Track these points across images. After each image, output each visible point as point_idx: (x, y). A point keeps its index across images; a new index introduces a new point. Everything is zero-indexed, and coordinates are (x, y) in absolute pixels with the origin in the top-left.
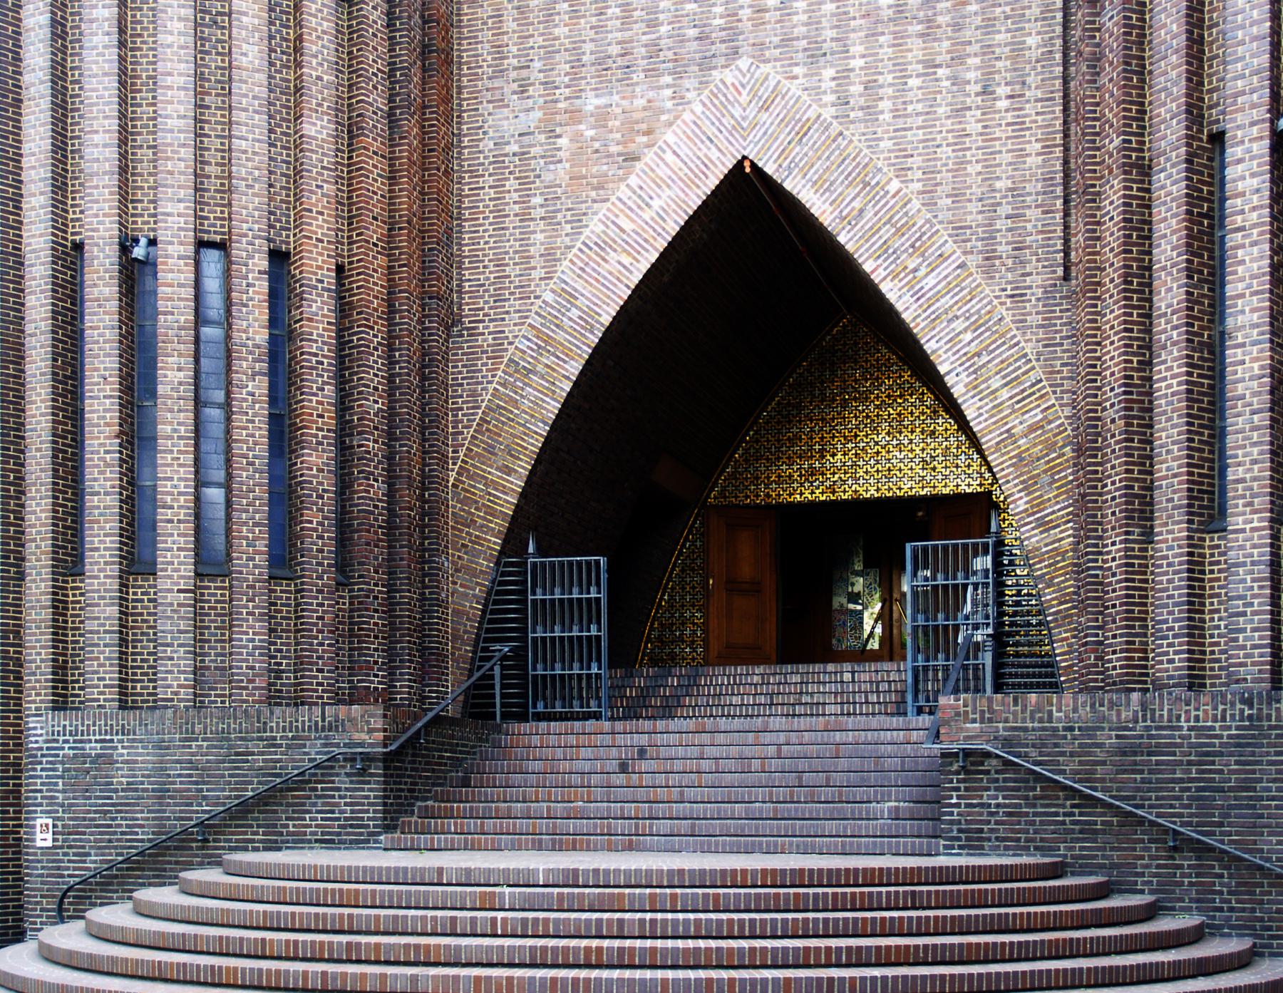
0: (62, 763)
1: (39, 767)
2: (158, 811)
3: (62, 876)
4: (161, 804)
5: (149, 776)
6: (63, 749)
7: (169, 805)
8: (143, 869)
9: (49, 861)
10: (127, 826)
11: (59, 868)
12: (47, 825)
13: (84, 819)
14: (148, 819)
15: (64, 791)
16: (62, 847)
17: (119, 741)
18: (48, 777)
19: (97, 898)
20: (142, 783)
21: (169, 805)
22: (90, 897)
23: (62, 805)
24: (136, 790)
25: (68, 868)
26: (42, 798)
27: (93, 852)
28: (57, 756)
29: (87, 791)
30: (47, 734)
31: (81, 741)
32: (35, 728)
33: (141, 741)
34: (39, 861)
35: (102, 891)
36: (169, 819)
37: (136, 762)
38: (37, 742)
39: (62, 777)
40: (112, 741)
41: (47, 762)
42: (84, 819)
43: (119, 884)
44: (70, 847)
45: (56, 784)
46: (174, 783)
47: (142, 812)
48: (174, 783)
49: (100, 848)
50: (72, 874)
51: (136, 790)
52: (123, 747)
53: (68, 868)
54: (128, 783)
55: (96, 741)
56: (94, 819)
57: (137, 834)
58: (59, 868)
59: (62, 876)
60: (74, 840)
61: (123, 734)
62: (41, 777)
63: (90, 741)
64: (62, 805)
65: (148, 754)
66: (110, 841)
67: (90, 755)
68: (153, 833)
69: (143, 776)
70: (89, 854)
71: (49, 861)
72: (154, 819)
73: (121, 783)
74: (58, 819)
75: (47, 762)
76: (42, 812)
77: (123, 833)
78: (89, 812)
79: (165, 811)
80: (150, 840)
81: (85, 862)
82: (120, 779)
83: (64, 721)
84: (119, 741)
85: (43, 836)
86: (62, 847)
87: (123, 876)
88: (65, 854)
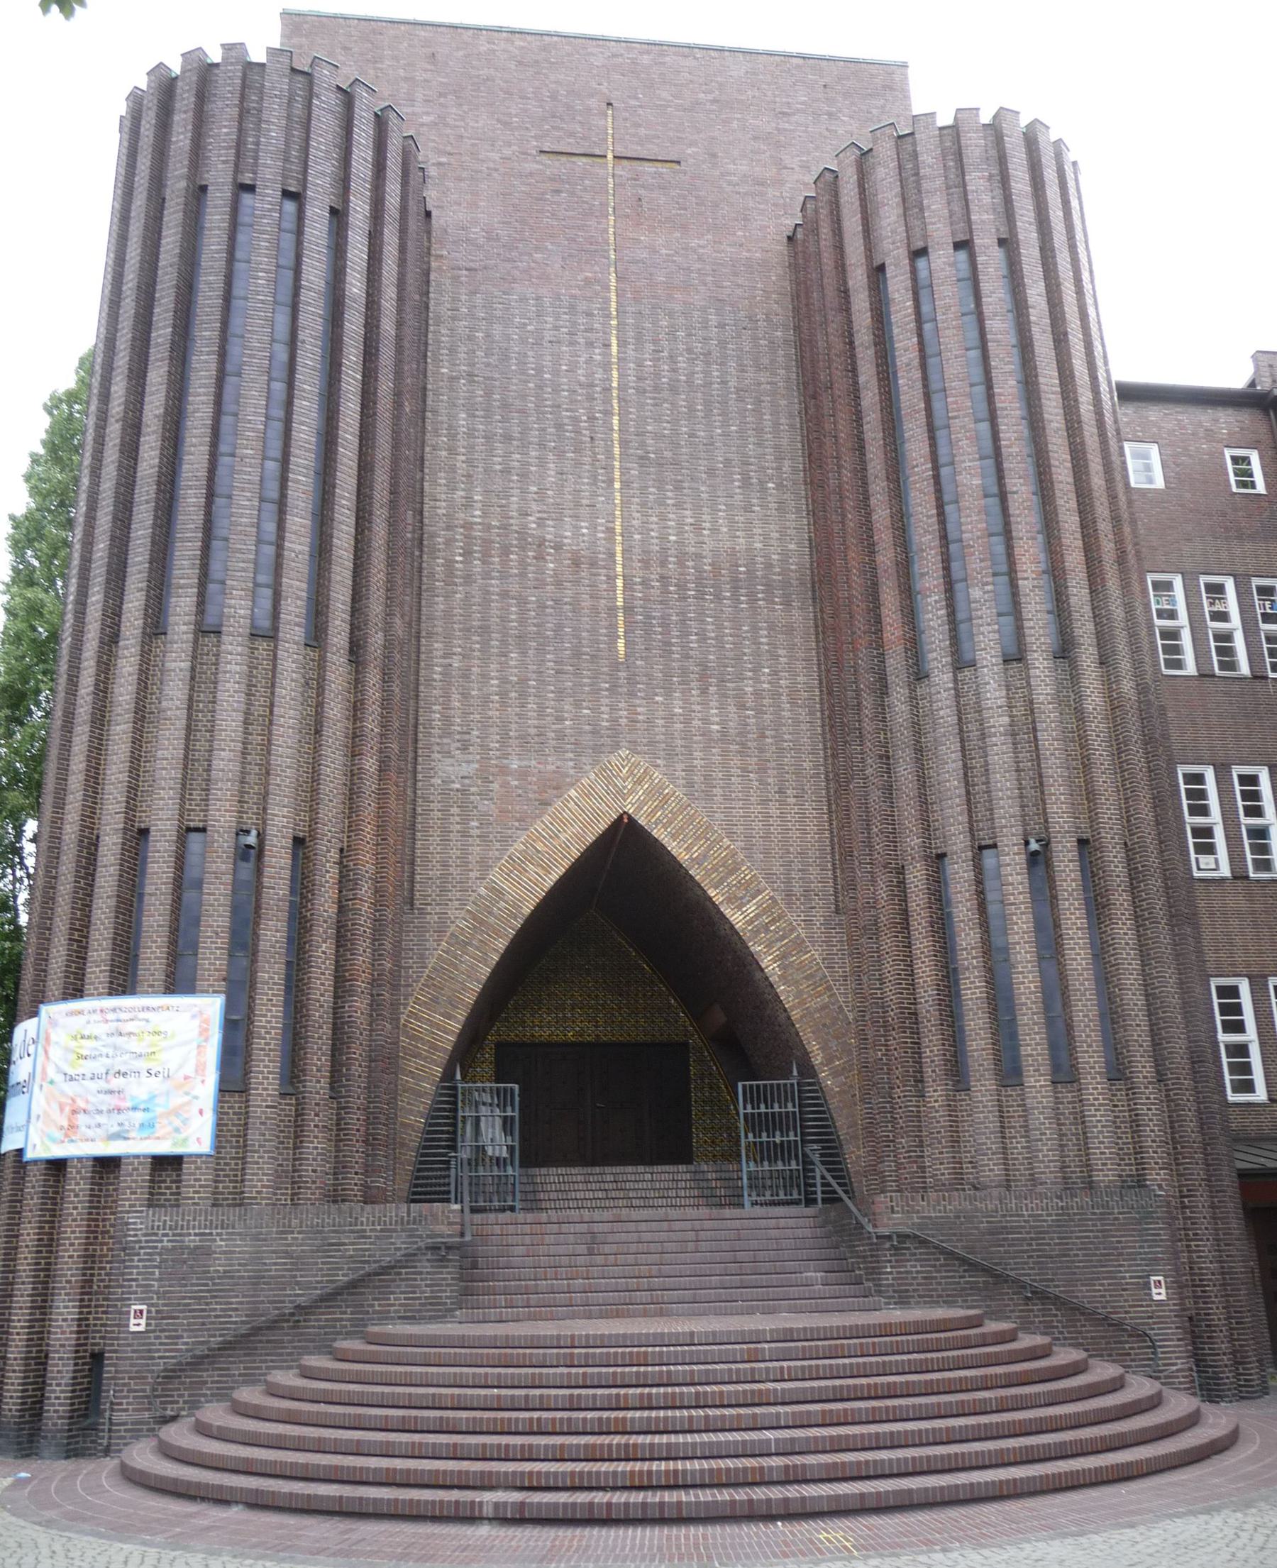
0: (160, 1254)
1: (136, 1258)
2: (253, 1296)
3: (153, 1358)
4: (255, 1290)
5: (246, 1265)
6: (162, 1241)
7: (263, 1290)
8: (234, 1349)
9: (140, 1345)
10: (222, 1310)
11: (149, 1351)
12: (141, 1312)
13: (179, 1305)
14: (241, 1303)
15: (160, 1280)
16: (154, 1331)
17: (218, 1234)
18: (145, 1267)
19: (186, 1377)
20: (239, 1271)
21: (263, 1290)
22: (180, 1377)
23: (157, 1293)
24: (232, 1277)
25: (159, 1351)
26: (137, 1286)
27: (185, 1334)
28: (156, 1247)
29: (184, 1279)
30: (147, 1228)
31: (180, 1235)
32: (135, 1223)
33: (240, 1234)
34: (129, 1345)
35: (192, 1370)
36: (263, 1302)
37: (234, 1252)
38: (136, 1235)
39: (158, 1267)
40: (211, 1234)
41: (145, 1254)
42: (179, 1305)
43: (210, 1363)
44: (161, 1331)
45: (153, 1273)
46: (270, 1270)
47: (237, 1296)
48: (270, 1270)
49: (192, 1331)
50: (165, 1355)
51: (232, 1277)
52: (222, 1240)
53: (159, 1351)
54: (225, 1272)
55: (196, 1235)
56: (189, 1304)
57: (230, 1316)
58: (149, 1351)
59: (153, 1358)
60: (167, 1324)
61: (222, 1228)
62: (137, 1267)
63: (190, 1235)
64: (157, 1293)
65: (246, 1246)
66: (203, 1324)
67: (188, 1247)
68: (247, 1316)
69: (240, 1265)
70: (182, 1337)
71: (140, 1345)
72: (248, 1303)
73: (218, 1271)
74: (153, 1305)
75: (145, 1254)
76: (136, 1299)
77: (216, 1317)
78: (184, 1298)
79: (259, 1296)
80: (242, 1322)
81: (176, 1344)
82: (218, 1266)
83: (164, 1217)
84: (218, 1234)
85: (137, 1321)
86: (154, 1331)
87: (214, 1356)
88: (157, 1338)
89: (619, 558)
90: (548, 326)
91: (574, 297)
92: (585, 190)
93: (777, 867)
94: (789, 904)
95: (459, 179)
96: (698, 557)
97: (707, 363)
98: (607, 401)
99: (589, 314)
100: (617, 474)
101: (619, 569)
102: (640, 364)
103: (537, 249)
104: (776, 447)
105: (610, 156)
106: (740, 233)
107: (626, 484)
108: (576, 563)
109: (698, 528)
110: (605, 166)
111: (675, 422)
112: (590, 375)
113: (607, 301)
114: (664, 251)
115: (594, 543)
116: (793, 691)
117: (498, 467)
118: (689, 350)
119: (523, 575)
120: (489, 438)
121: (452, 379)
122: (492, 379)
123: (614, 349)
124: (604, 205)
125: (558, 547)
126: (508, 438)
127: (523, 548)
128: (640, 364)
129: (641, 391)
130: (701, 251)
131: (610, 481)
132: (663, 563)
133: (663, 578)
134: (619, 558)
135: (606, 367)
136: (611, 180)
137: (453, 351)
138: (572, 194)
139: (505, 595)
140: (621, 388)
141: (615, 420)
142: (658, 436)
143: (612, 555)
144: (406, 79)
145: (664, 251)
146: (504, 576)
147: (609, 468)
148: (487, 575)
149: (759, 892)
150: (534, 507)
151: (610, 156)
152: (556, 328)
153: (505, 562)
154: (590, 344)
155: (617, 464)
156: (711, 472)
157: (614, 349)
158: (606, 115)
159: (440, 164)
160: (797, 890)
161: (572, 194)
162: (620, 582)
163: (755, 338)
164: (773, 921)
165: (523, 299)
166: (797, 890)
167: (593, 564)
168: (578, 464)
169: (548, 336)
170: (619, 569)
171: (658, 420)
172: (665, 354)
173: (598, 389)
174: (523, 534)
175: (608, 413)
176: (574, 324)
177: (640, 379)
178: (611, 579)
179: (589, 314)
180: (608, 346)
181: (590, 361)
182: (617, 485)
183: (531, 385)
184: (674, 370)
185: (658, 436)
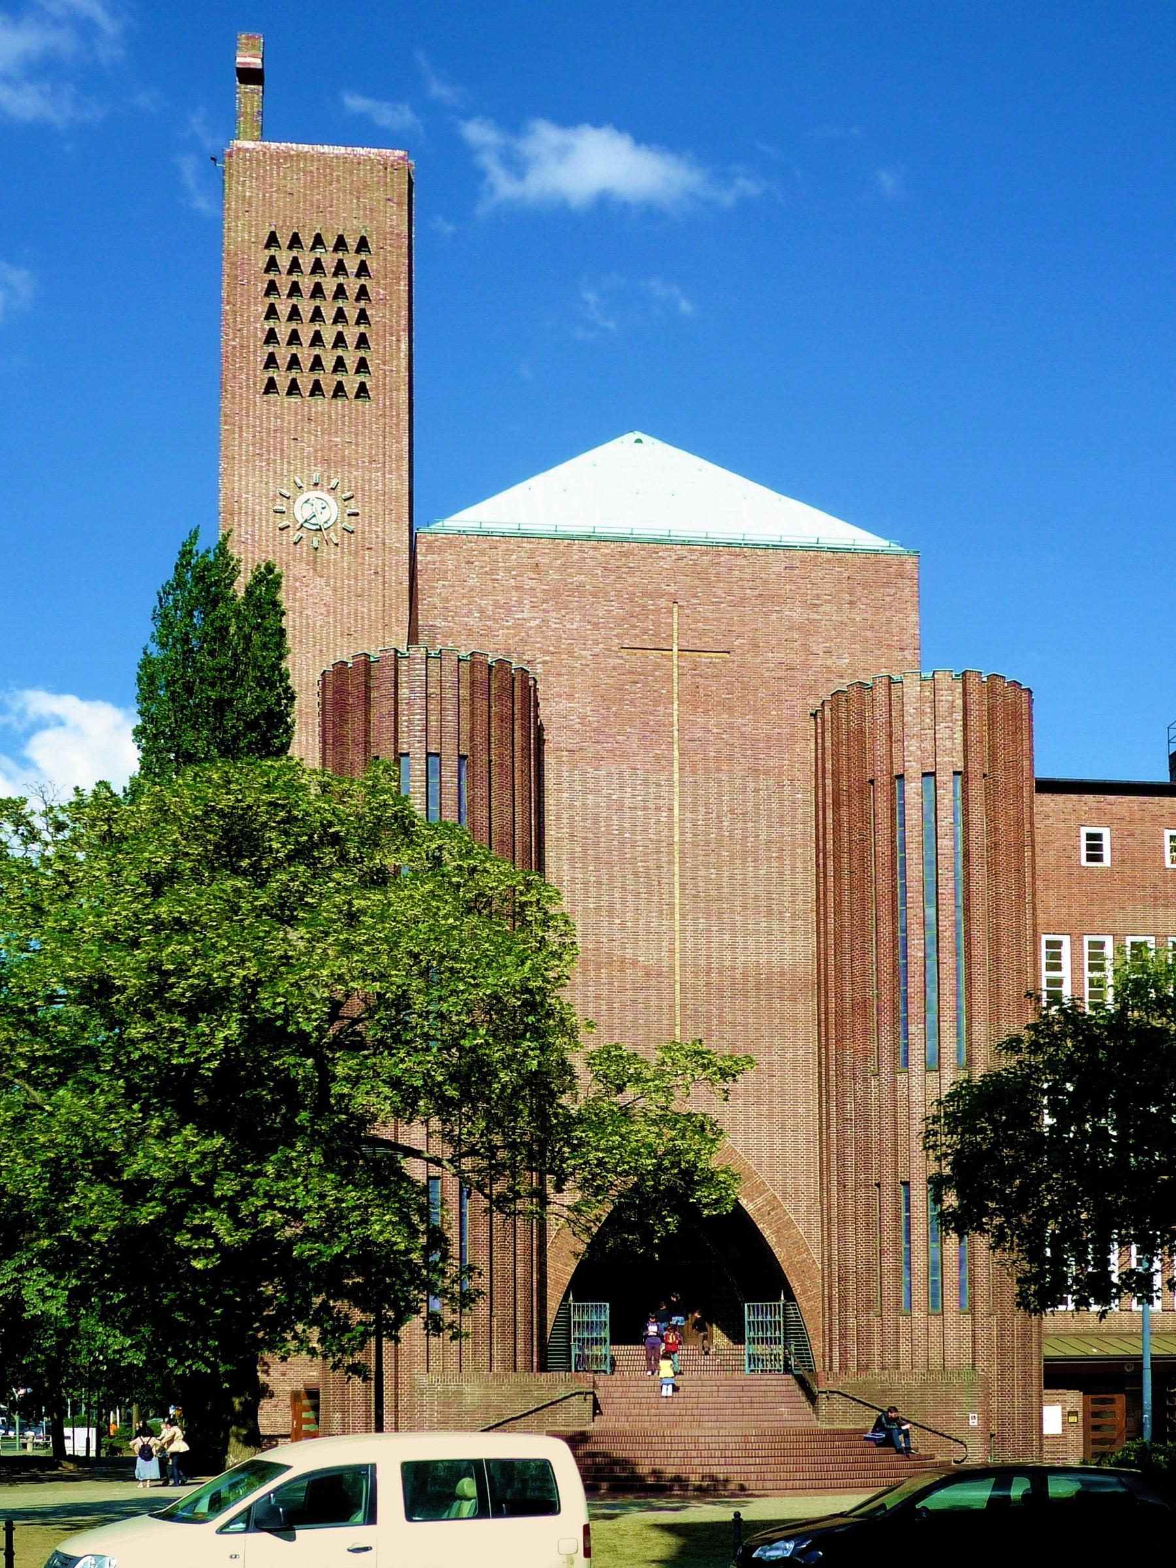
89: (677, 969)
90: (628, 795)
91: (646, 771)
92: (655, 680)
93: (778, 1177)
94: (784, 1199)
95: (560, 674)
96: (734, 968)
97: (745, 821)
98: (671, 854)
99: (658, 785)
100: (677, 908)
101: (677, 978)
102: (694, 822)
103: (619, 733)
104: (793, 886)
105: (675, 649)
106: (774, 713)
107: (683, 916)
108: (647, 975)
109: (733, 948)
110: (670, 659)
111: (719, 868)
112: (658, 833)
113: (672, 774)
114: (715, 731)
115: (660, 960)
116: (794, 1062)
117: (591, 906)
118: (732, 811)
119: (611, 984)
120: (585, 884)
121: (558, 840)
122: (586, 838)
123: (676, 811)
124: (670, 692)
125: (635, 963)
126: (599, 883)
127: (610, 964)
128: (694, 822)
129: (695, 845)
130: (743, 729)
131: (673, 914)
132: (708, 973)
133: (708, 984)
134: (677, 969)
135: (670, 826)
136: (675, 670)
137: (558, 818)
138: (646, 684)
139: (598, 997)
140: (682, 842)
141: (676, 868)
142: (707, 880)
143: (672, 969)
144: (517, 588)
145: (715, 731)
146: (597, 981)
147: (671, 905)
148: (586, 985)
149: (765, 1191)
150: (618, 935)
151: (675, 649)
152: (634, 797)
153: (598, 976)
154: (658, 809)
155: (677, 901)
156: (745, 906)
157: (676, 811)
158: (672, 612)
159: (545, 662)
160: (790, 1191)
161: (646, 684)
162: (678, 986)
163: (781, 800)
164: (773, 1209)
165: (609, 774)
166: (790, 1191)
167: (659, 975)
168: (649, 901)
169: (627, 802)
170: (677, 978)
171: (707, 866)
172: (714, 815)
173: (664, 844)
174: (609, 955)
175: (671, 863)
176: (647, 793)
177: (695, 835)
178: (672, 986)
179: (658, 785)
180: (671, 810)
181: (658, 822)
182: (677, 917)
183: (615, 843)
184: (720, 828)
185: (707, 880)
